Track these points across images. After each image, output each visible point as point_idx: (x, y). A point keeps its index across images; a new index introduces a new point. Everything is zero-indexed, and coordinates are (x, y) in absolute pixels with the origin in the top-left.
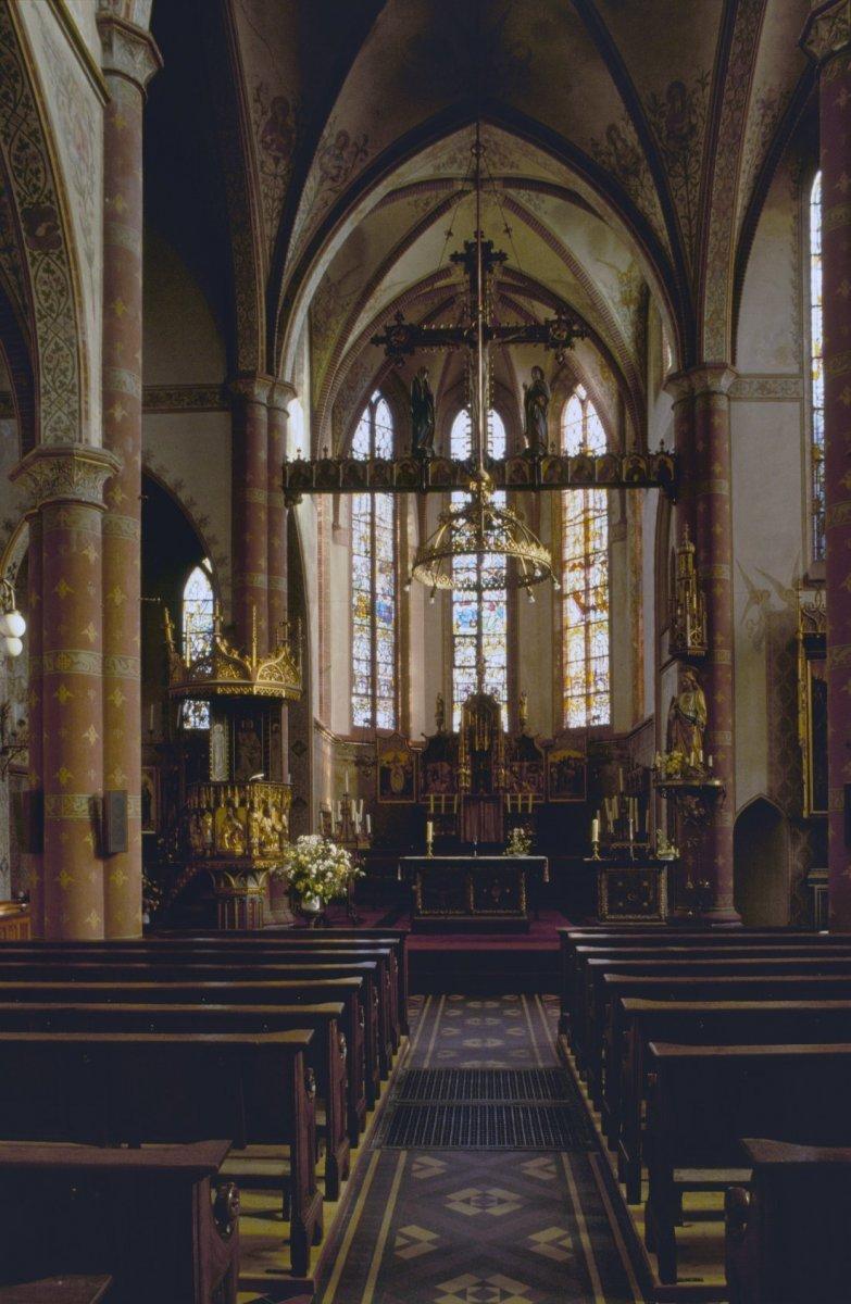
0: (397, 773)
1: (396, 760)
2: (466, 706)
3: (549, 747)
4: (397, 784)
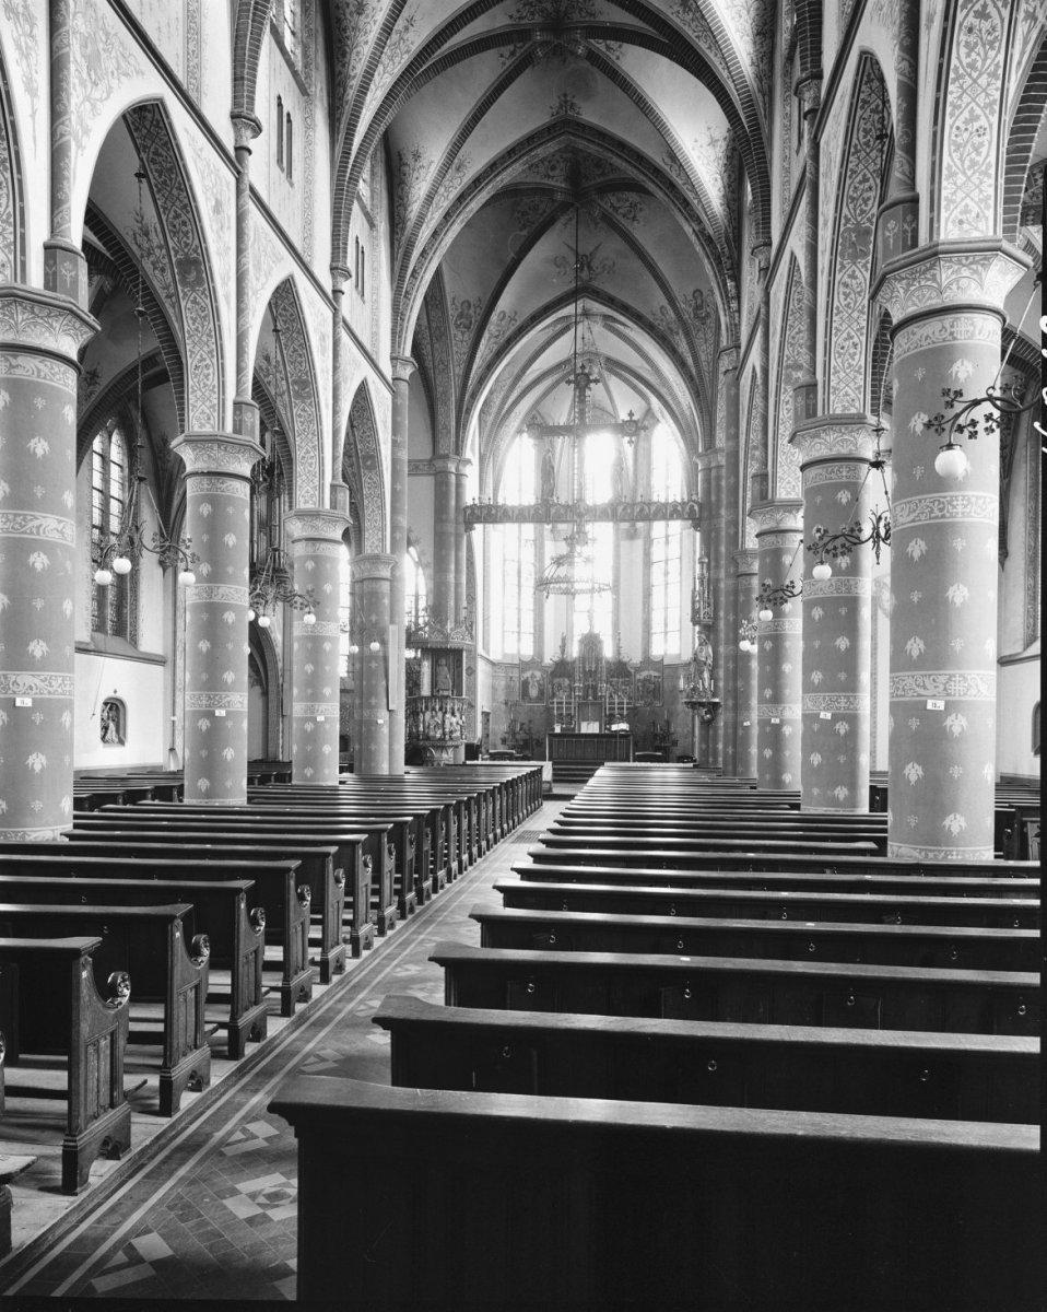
0: (534, 685)
1: (533, 676)
2: (581, 642)
3: (638, 670)
4: (534, 692)
